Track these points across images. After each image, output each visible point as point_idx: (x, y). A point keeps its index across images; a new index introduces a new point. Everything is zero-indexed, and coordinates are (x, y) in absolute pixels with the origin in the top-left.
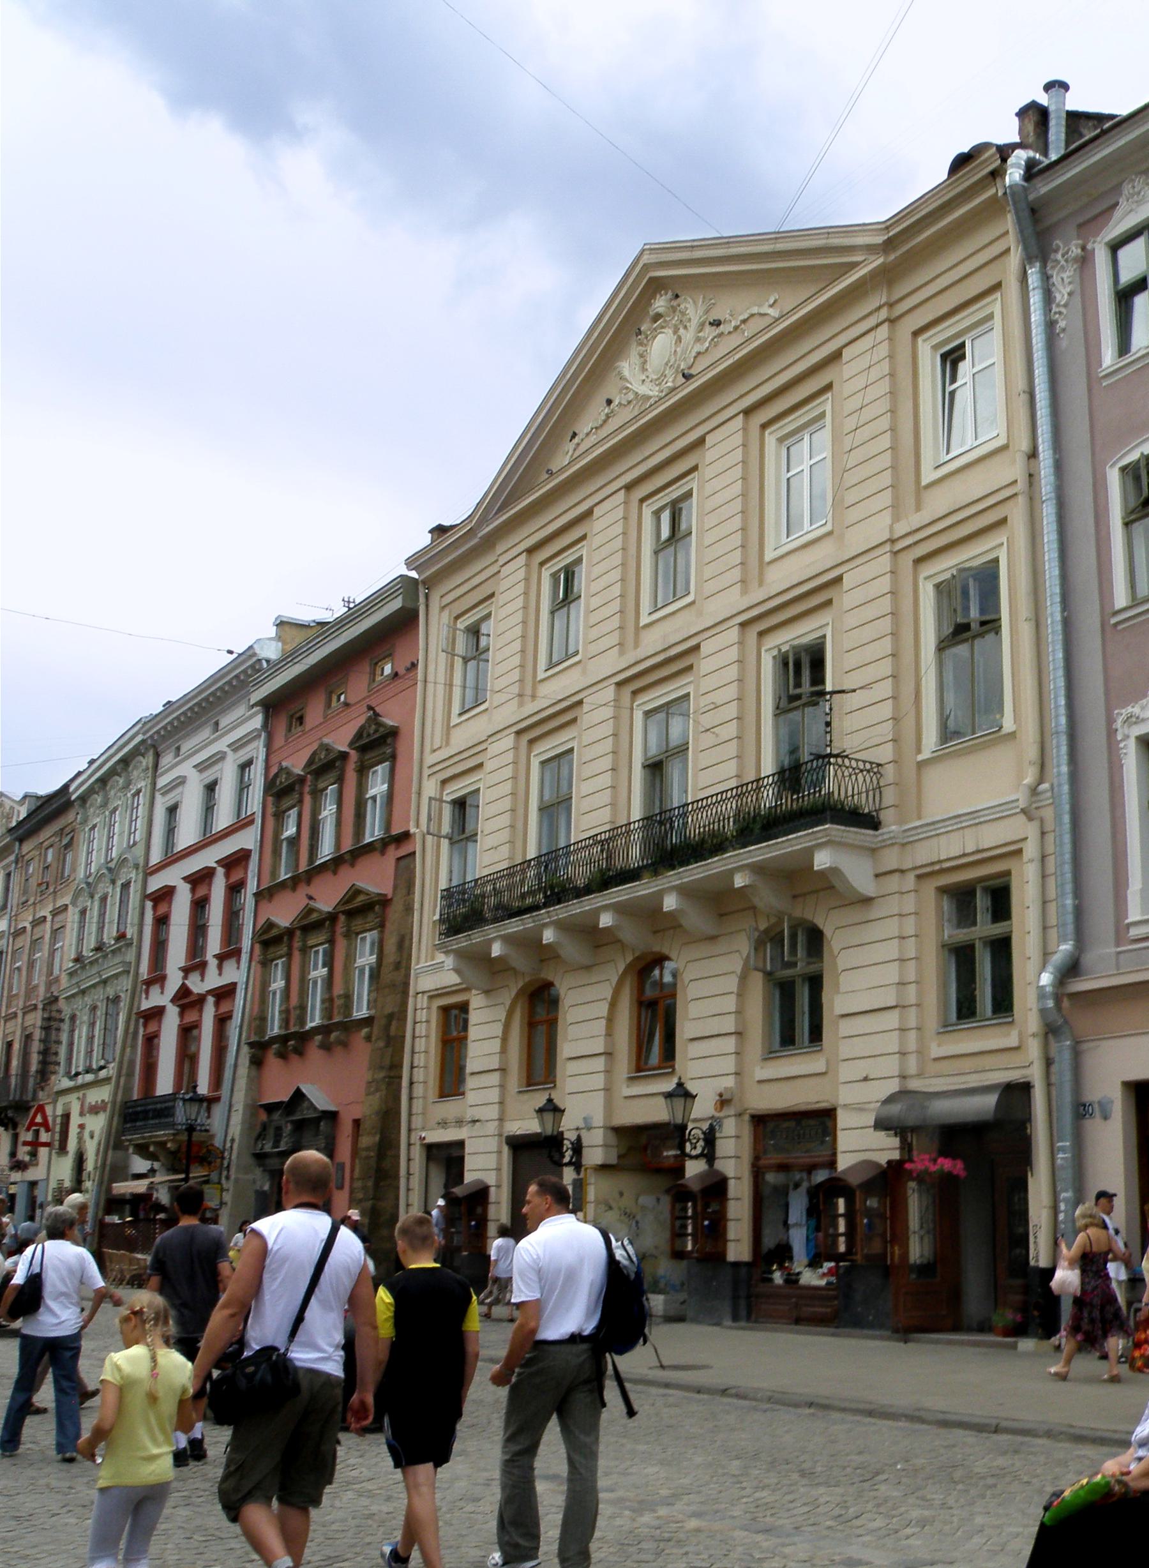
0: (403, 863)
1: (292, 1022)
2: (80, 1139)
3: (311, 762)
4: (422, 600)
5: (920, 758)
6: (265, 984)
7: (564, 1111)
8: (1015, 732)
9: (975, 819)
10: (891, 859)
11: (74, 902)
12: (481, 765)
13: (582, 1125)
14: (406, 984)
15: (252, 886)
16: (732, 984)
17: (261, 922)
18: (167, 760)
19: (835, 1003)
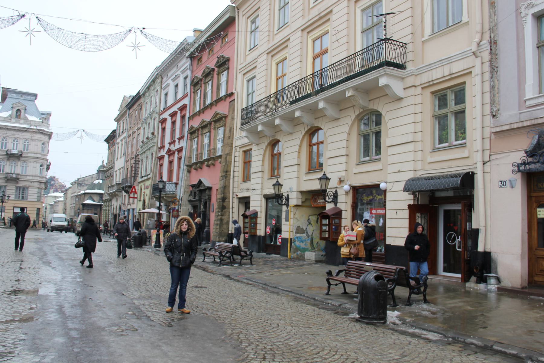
0: (231, 103)
1: (199, 158)
2: (144, 196)
3: (203, 73)
4: (236, 13)
5: (423, 39)
6: (191, 147)
7: (282, 185)
8: (468, 22)
9: (449, 61)
10: (410, 81)
11: (142, 126)
12: (256, 67)
13: (289, 191)
14: (232, 144)
15: (187, 116)
16: (345, 136)
17: (190, 126)
18: (164, 80)
19: (385, 141)
